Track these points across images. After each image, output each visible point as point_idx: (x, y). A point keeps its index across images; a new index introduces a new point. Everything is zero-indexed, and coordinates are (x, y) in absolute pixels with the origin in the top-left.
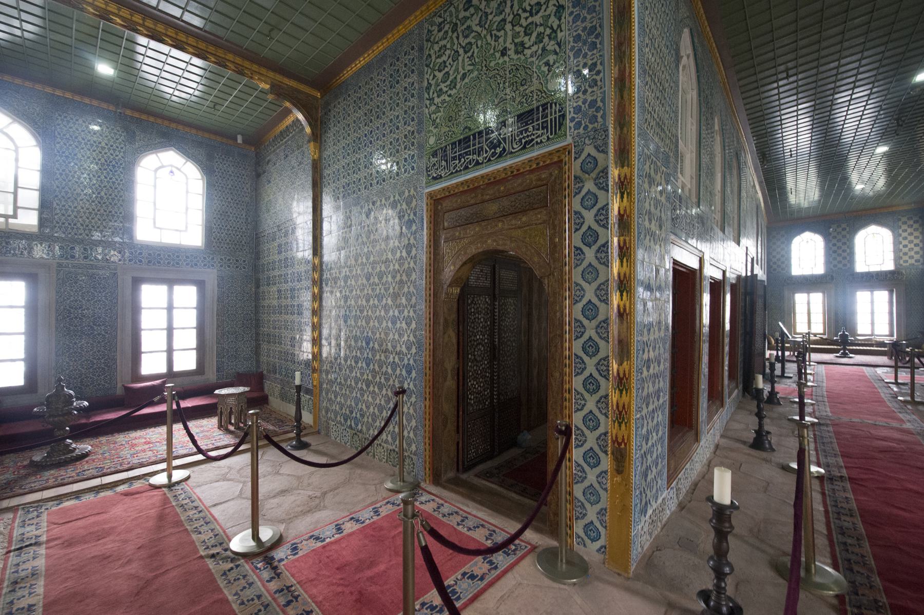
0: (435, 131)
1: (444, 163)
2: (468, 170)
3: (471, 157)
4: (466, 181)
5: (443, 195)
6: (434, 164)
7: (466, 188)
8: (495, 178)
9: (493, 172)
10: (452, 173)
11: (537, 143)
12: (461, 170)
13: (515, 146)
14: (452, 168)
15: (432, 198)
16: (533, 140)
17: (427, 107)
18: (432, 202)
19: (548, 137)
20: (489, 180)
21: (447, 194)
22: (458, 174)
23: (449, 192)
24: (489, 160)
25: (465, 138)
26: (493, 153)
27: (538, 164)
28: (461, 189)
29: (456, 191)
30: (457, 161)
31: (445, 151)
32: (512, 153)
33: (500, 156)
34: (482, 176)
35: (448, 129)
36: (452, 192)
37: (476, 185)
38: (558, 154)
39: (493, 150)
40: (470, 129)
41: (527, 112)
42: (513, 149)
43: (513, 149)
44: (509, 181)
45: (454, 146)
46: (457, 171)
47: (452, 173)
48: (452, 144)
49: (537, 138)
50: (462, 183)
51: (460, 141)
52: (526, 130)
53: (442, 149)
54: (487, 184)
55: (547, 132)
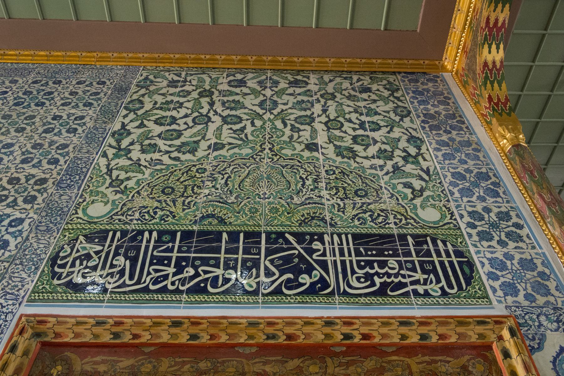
0: (112, 197)
1: (121, 261)
2: (202, 297)
3: (219, 272)
4: (195, 322)
5: (88, 338)
6: (88, 257)
7: (184, 339)
8: (289, 337)
9: (290, 322)
10: (146, 290)
11: (416, 293)
12: (177, 291)
13: (355, 284)
14: (147, 280)
15: (37, 335)
16: (405, 285)
17: (105, 155)
18: (35, 345)
19: (442, 288)
20: (274, 337)
21: (107, 338)
22: (169, 297)
23: (116, 335)
24: (277, 292)
25: (201, 233)
26: (289, 280)
27: (424, 337)
28: (165, 338)
29: (146, 337)
30: (171, 270)
31: (133, 239)
32: (345, 293)
33: (312, 290)
34: (253, 323)
35: (156, 204)
36: (127, 338)
37: (224, 338)
38: (480, 329)
39: (291, 276)
40: (222, 221)
41: (375, 235)
42: (350, 286)
43: (350, 286)
44: (337, 355)
45: (166, 238)
46: (164, 290)
47: (146, 290)
48: (161, 233)
49: (412, 283)
50: (176, 323)
51: (187, 235)
52: (383, 265)
53: (124, 233)
54: (258, 345)
55: (438, 281)
